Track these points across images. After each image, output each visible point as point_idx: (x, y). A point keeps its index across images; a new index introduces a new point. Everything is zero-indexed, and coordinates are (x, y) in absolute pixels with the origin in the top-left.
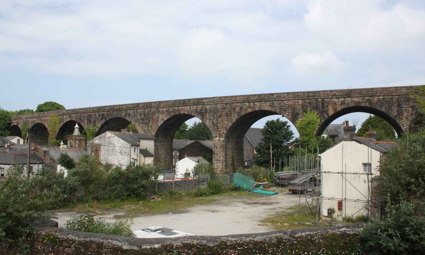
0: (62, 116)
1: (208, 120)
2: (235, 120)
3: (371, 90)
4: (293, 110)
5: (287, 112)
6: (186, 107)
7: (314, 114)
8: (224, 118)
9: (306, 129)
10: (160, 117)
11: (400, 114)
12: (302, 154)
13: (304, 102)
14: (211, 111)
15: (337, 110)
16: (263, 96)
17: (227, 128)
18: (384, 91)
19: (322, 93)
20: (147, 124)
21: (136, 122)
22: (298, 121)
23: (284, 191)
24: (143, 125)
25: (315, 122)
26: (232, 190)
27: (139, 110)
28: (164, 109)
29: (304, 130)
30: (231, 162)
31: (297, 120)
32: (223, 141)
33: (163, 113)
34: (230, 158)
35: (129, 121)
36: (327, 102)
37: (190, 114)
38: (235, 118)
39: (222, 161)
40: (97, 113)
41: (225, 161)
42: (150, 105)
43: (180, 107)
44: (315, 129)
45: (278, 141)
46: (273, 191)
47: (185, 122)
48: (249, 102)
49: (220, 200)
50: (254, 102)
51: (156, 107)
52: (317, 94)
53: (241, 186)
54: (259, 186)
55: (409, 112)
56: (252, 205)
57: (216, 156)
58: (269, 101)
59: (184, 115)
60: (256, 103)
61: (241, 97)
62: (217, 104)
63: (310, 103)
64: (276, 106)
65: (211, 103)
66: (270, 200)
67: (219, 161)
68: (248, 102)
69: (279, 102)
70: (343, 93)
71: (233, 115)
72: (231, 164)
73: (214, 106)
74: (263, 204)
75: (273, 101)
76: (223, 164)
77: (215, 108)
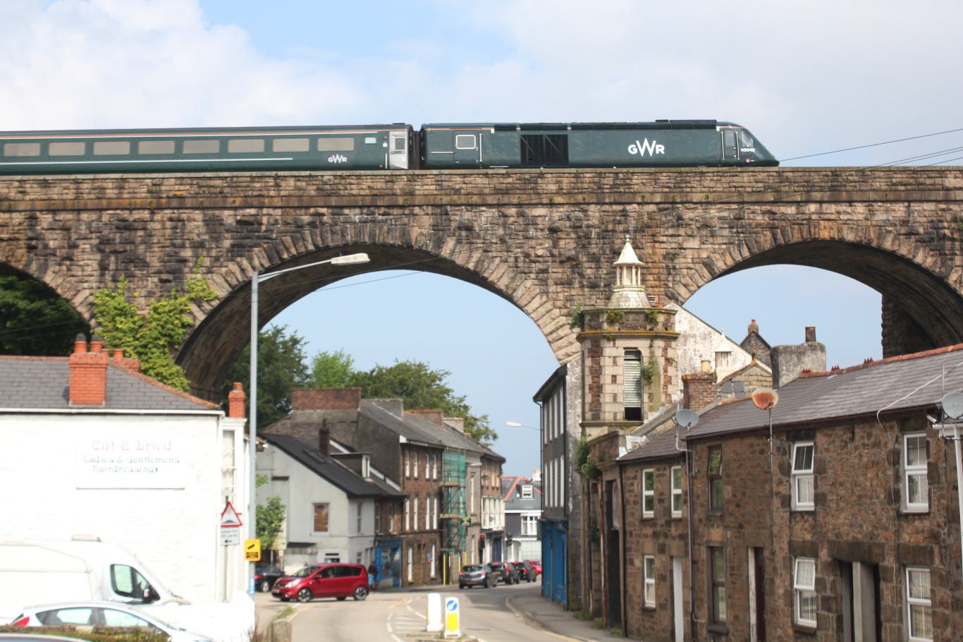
10: (689, 254)
24: (573, 292)
33: (704, 232)
37: (870, 241)
40: (198, 215)
42: (614, 186)
43: (813, 207)
51: (658, 198)
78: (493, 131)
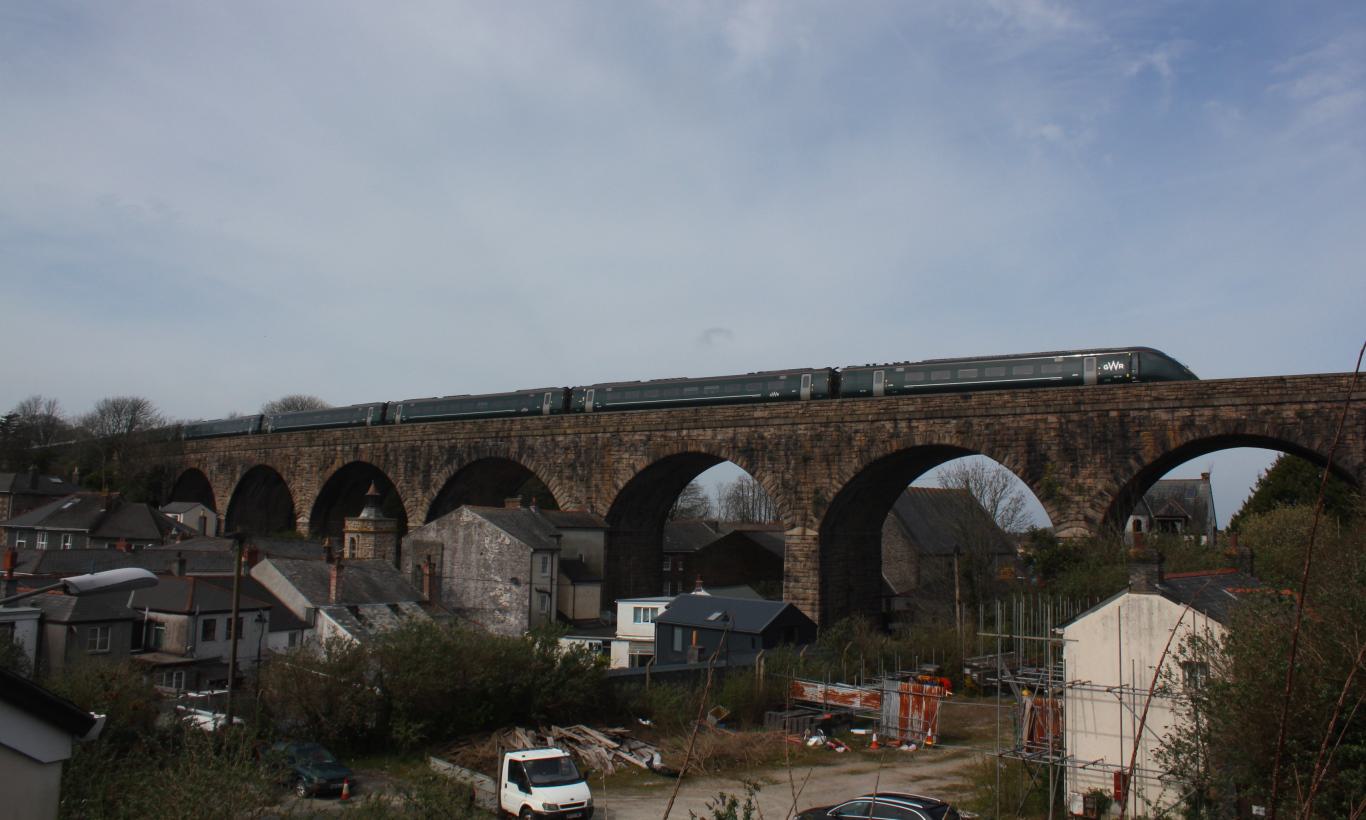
0: (332, 447)
1: (768, 472)
2: (852, 475)
3: (1276, 385)
6: (701, 432)
8: (819, 468)
14: (778, 444)
18: (1320, 386)
19: (1120, 392)
20: (586, 481)
21: (551, 473)
27: (561, 438)
28: (637, 437)
33: (632, 449)
35: (528, 471)
36: (1137, 421)
38: (851, 465)
39: (810, 601)
43: (685, 432)
47: (693, 482)
48: (895, 420)
50: (910, 420)
51: (611, 429)
57: (792, 584)
58: (954, 418)
59: (698, 454)
60: (914, 424)
62: (798, 424)
63: (1080, 424)
65: (777, 421)
67: (801, 602)
73: (786, 430)
77: (790, 437)
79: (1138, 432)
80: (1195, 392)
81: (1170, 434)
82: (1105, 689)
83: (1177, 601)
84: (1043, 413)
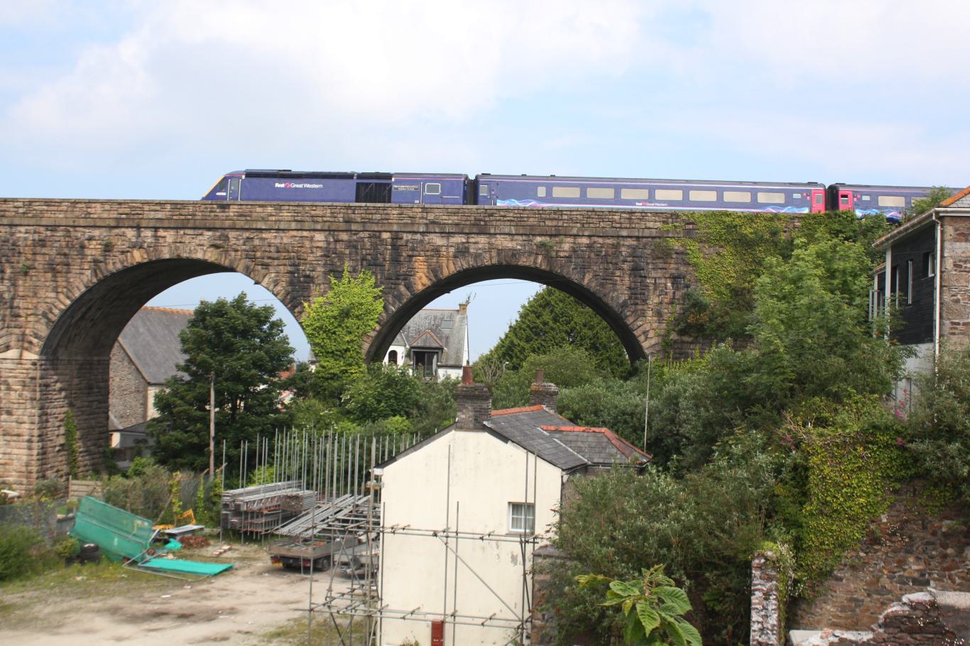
2: (83, 289)
3: (553, 216)
4: (294, 265)
5: (272, 269)
7: (363, 282)
8: (43, 279)
9: (334, 333)
11: (636, 298)
12: (319, 422)
13: (332, 240)
15: (442, 273)
16: (191, 209)
17: (50, 316)
18: (594, 221)
19: (395, 212)
22: (309, 306)
23: (255, 559)
25: (368, 312)
26: (69, 561)
29: (330, 338)
30: (62, 440)
31: (305, 301)
32: (34, 364)
34: (59, 426)
38: (81, 280)
39: (26, 438)
41: (39, 436)
44: (365, 334)
45: (237, 378)
46: (217, 559)
48: (138, 228)
49: (26, 606)
50: (156, 229)
52: (378, 217)
53: (102, 541)
54: (167, 542)
55: (666, 294)
56: (146, 626)
58: (209, 229)
60: (161, 233)
61: (107, 207)
62: (16, 225)
63: (351, 245)
64: (235, 247)
66: (206, 598)
67: (15, 438)
68: (135, 225)
69: (246, 234)
70: (464, 218)
71: (75, 269)
72: (62, 445)
74: (184, 617)
75: (225, 229)
76: (30, 448)
78: (244, 177)
79: (411, 256)
80: (473, 218)
81: (444, 260)
82: (432, 533)
83: (505, 439)
84: (310, 230)
